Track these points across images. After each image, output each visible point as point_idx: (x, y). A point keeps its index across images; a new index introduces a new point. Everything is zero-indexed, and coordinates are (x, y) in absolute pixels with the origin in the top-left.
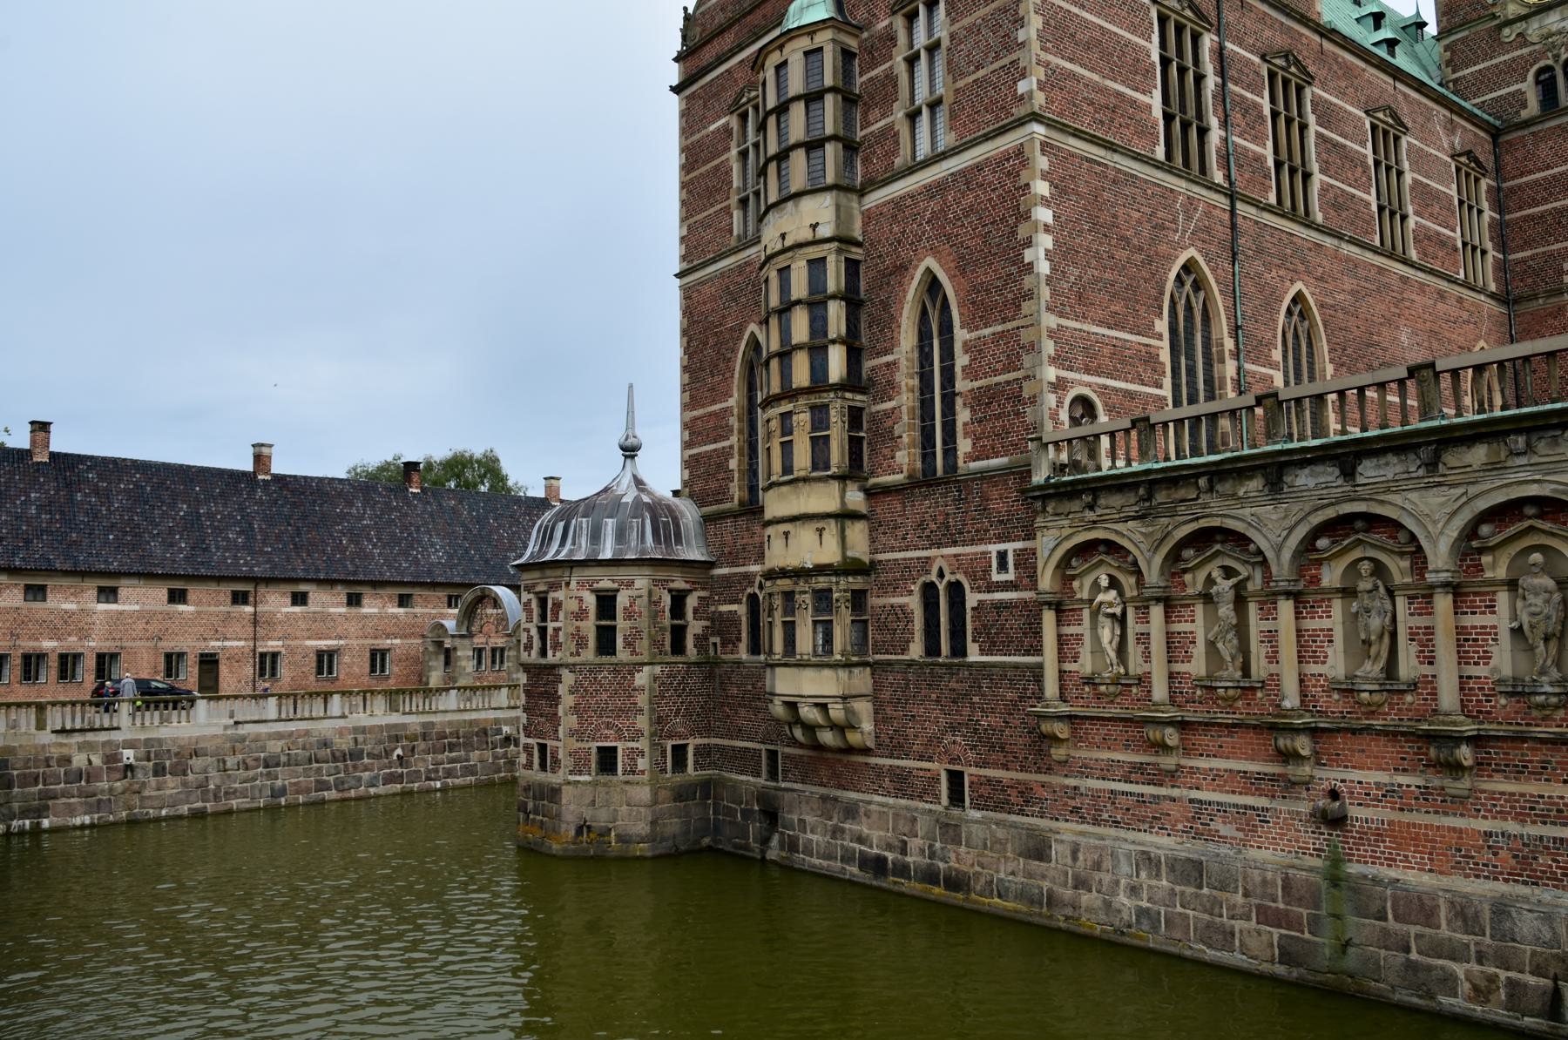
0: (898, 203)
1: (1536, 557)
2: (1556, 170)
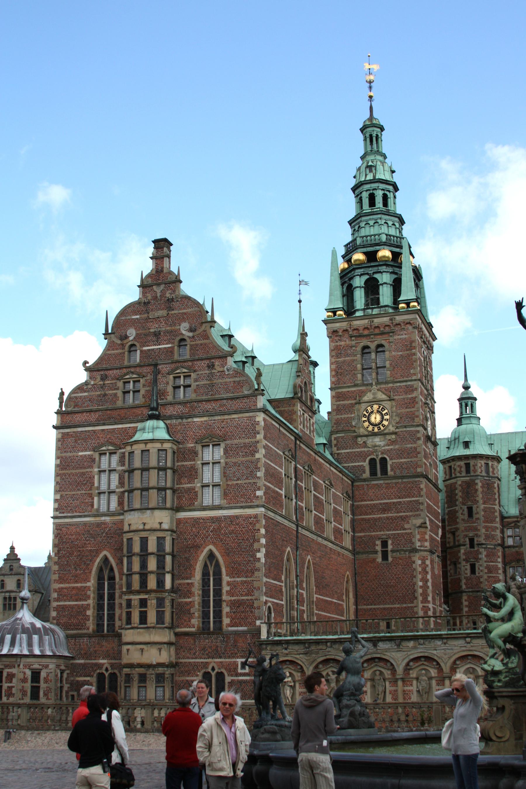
0: (196, 521)
1: (423, 672)
2: (375, 502)
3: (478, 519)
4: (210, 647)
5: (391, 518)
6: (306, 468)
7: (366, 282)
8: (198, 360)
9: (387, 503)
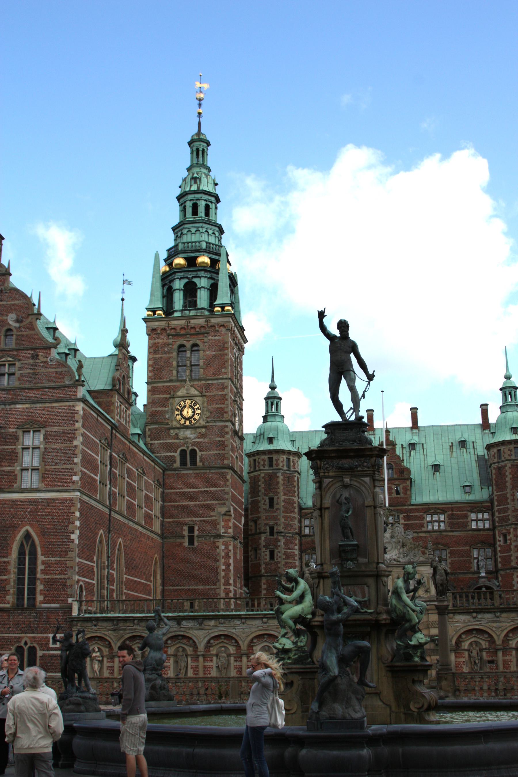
0: (14, 502)
1: (223, 649)
3: (278, 509)
4: (24, 623)
5: (199, 506)
6: (121, 456)
7: (186, 285)
8: (24, 350)
9: (195, 492)
